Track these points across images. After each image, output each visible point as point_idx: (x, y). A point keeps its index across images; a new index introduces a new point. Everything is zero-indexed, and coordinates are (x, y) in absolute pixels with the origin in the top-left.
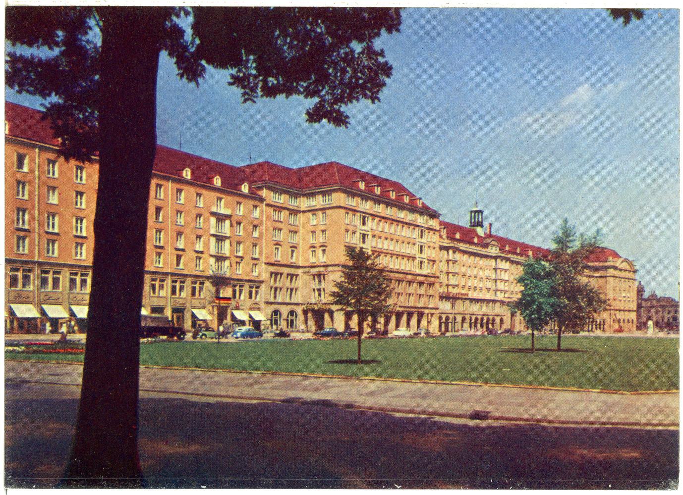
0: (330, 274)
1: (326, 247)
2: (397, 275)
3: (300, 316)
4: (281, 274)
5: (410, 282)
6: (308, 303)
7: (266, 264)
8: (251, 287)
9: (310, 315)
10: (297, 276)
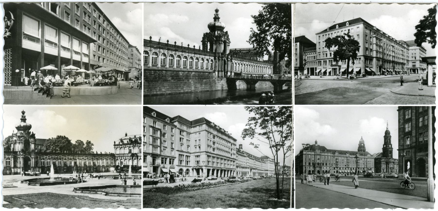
3: (191, 171)
4: (183, 155)
5: (228, 160)
8: (170, 159)
10: (190, 156)
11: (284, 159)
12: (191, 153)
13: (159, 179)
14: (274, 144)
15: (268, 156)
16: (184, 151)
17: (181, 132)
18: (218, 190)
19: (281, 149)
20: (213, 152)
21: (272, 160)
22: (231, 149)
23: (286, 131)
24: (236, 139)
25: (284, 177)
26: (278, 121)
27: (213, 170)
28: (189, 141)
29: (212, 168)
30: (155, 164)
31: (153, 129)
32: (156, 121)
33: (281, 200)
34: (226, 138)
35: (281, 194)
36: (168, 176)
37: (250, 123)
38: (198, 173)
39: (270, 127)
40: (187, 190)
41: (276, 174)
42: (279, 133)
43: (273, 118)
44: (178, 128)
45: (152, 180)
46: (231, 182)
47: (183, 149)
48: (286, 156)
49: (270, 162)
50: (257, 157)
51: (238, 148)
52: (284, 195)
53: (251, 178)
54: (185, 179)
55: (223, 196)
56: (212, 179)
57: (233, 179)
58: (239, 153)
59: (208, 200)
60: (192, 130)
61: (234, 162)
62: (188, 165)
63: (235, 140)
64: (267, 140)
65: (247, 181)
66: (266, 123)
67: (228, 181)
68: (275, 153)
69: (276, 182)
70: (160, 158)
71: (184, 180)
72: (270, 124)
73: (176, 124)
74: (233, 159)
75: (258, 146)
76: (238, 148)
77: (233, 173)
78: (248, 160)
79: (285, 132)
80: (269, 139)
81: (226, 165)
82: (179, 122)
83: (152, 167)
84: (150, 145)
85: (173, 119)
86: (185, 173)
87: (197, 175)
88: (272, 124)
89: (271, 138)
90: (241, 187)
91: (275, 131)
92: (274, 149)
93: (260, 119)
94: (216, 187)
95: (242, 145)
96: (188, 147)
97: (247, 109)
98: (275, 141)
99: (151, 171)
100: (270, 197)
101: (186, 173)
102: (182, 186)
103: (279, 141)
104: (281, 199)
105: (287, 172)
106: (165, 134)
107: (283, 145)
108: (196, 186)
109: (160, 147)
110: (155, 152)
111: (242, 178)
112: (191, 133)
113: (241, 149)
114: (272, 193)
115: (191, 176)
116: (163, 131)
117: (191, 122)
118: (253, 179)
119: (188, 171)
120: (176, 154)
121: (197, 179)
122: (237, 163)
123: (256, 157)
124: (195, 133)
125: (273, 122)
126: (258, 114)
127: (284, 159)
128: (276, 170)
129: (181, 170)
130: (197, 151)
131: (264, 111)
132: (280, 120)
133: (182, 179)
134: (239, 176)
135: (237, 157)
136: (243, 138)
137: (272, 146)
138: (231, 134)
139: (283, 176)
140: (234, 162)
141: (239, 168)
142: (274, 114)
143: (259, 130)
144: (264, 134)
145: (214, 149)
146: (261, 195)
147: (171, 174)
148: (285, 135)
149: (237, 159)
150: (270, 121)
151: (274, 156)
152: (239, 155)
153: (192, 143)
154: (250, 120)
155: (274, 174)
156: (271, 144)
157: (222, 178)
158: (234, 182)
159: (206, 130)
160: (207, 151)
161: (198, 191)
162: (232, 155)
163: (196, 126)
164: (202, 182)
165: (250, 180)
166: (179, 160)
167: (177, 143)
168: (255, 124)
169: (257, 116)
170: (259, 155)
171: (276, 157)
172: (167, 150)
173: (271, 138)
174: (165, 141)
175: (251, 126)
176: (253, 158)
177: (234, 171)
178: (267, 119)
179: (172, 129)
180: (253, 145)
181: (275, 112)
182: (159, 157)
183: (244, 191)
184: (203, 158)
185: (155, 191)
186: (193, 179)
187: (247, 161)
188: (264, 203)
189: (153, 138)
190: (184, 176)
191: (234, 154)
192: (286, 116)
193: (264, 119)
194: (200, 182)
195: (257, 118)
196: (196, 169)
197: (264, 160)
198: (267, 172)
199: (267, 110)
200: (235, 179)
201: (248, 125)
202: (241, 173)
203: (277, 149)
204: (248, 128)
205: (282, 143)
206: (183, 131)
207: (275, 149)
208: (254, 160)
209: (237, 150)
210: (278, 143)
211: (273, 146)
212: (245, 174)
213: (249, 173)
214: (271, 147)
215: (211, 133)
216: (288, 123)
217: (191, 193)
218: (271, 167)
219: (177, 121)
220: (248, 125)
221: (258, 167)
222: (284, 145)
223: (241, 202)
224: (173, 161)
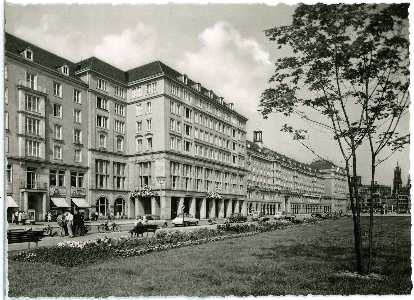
0: (157, 161)
1: (152, 135)
2: (216, 167)
5: (226, 173)
6: (135, 191)
7: (91, 150)
8: (73, 173)
9: (137, 200)
10: (124, 165)
11: (373, 167)
12: (127, 156)
13: (45, 226)
14: (344, 127)
15: (330, 159)
16: (110, 150)
17: (99, 99)
18: (201, 253)
19: (366, 140)
20: (185, 152)
21: (341, 172)
22: (234, 144)
23: (376, 92)
24: (248, 119)
25: (375, 214)
26: (355, 67)
27: (187, 201)
28: (123, 123)
29: (183, 195)
30: (34, 186)
31: (26, 95)
32: (33, 70)
33: (367, 277)
34: (218, 114)
35: (366, 261)
36: (70, 217)
37: (281, 74)
38: (147, 209)
39: (334, 83)
40: (118, 254)
41: (352, 207)
42: (357, 97)
44: (91, 91)
45: (27, 228)
46: (235, 230)
47: (105, 147)
48: (376, 158)
49: (337, 176)
50: (303, 165)
51: (252, 140)
52: (374, 263)
53: (286, 218)
54: (114, 225)
55: (214, 267)
56: (185, 224)
57: (239, 224)
59: (174, 279)
61: (241, 176)
62: (121, 189)
63: (243, 120)
64: (326, 119)
65: (276, 227)
67: (228, 229)
68: (348, 152)
69: (353, 228)
70: (47, 171)
71: (110, 228)
72: (334, 76)
73: (87, 79)
74: (239, 169)
75: (303, 134)
76: (251, 139)
77: (240, 208)
78: (277, 171)
79: (375, 96)
80: (332, 116)
81: (221, 187)
82: (95, 75)
83: (26, 197)
84: (19, 135)
85: (79, 66)
86: (113, 210)
88: (339, 76)
89: (337, 112)
90: (262, 242)
91: (348, 94)
92: (346, 142)
93: (306, 62)
94: (196, 244)
96: (119, 141)
97: (271, 36)
98: (347, 122)
99: (22, 205)
100: (337, 269)
101: (115, 208)
102: (105, 244)
103: (358, 119)
104: (367, 274)
105: (380, 202)
106: (59, 107)
107: (368, 131)
108: (143, 244)
109: (46, 141)
110: (32, 155)
111: (264, 220)
112: (126, 104)
113: (259, 144)
114: (344, 257)
115: (129, 216)
116: (53, 100)
117: (126, 74)
118: (293, 222)
119: (119, 205)
121: (143, 222)
122: (249, 181)
123: (298, 163)
124: (138, 102)
125: (341, 70)
126: (301, 48)
127: (373, 167)
128: (351, 197)
131: (317, 40)
132: (360, 64)
133: (106, 225)
134: (255, 216)
135: (249, 164)
136: (263, 114)
137: (339, 133)
138: (232, 104)
139: (371, 213)
140: (241, 176)
141: (254, 192)
142: (342, 47)
144: (319, 102)
145: (188, 144)
146: (313, 265)
147: (75, 212)
148: (375, 105)
149: (249, 169)
150: (333, 69)
151: (347, 161)
152: (254, 158)
154: (281, 67)
155: (348, 209)
156: (337, 128)
157: (210, 221)
158: (242, 229)
159: (165, 95)
160: (168, 150)
161: (149, 255)
162: (237, 159)
163: (138, 85)
164: (158, 231)
165: (285, 225)
166: (97, 175)
167: (89, 129)
168: (294, 77)
169: (300, 55)
170: (307, 158)
171: (351, 162)
172: (65, 147)
173: (337, 112)
174: (59, 126)
175: (285, 81)
176: (291, 166)
177: (242, 202)
178: (326, 63)
179: (77, 92)
180: (291, 131)
181: (345, 42)
182: (43, 168)
185: (35, 259)
186: (136, 225)
187: (277, 175)
188: (321, 286)
189: (26, 118)
190: (109, 218)
191: (241, 157)
192: (374, 52)
193: (318, 63)
194: (154, 231)
195: (300, 60)
196: (140, 198)
197: (321, 171)
198: (327, 202)
199: (324, 37)
200: (245, 224)
201: (275, 78)
202: (259, 206)
204: (276, 88)
205: (366, 126)
206: (107, 98)
207: (350, 141)
208: (293, 170)
209: (249, 146)
210: (357, 126)
211: (344, 134)
212: (271, 207)
213: (283, 206)
214: (337, 137)
216: (381, 73)
217: (127, 264)
220: (275, 78)
221: (305, 189)
223: (263, 283)
224: (80, 179)
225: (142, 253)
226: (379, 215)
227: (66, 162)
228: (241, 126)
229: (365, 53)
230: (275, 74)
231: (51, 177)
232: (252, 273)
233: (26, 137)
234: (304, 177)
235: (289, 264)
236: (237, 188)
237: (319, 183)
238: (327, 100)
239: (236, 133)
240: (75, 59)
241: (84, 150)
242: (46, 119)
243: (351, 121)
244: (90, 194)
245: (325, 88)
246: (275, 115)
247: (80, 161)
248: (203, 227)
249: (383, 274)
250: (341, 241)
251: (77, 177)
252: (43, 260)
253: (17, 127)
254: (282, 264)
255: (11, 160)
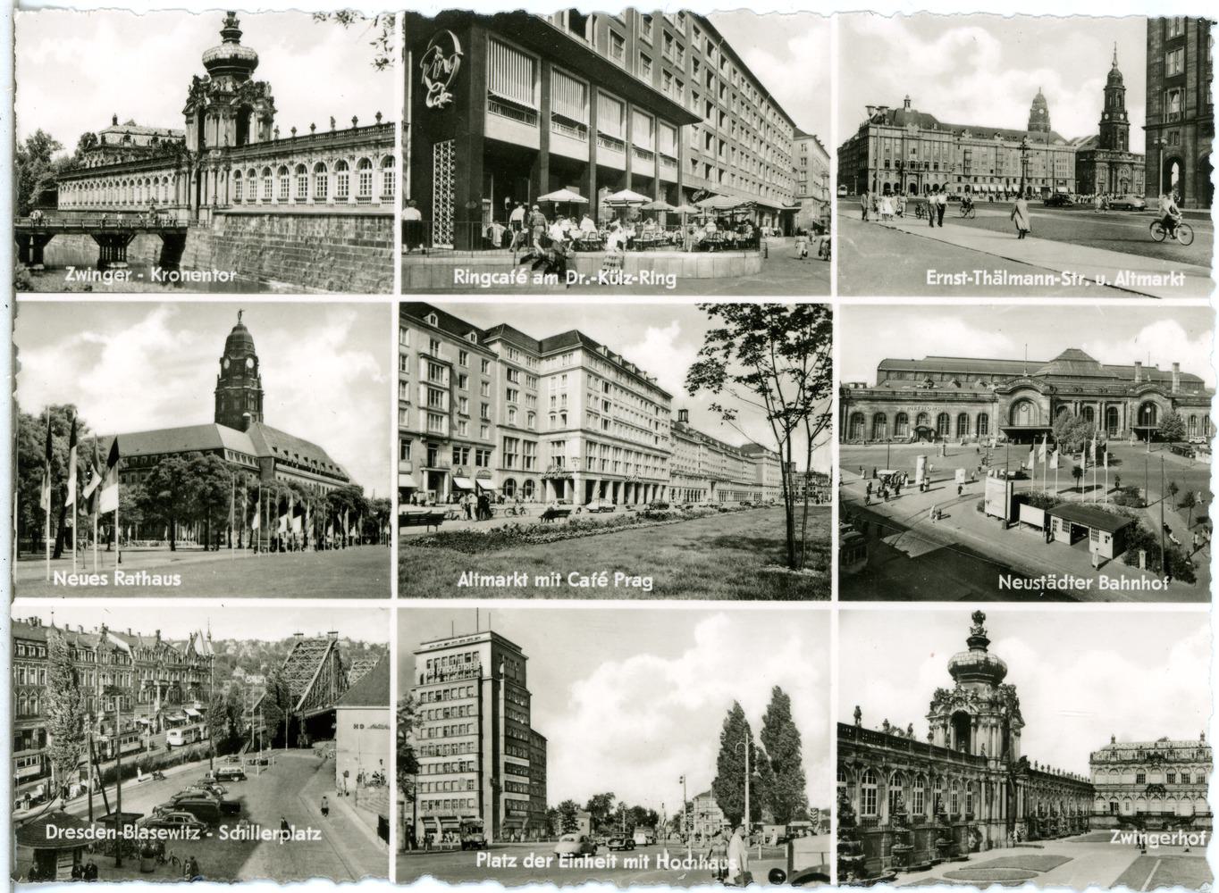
3: (539, 485)
8: (479, 452)
9: (548, 483)
10: (535, 443)
11: (810, 452)
12: (538, 434)
14: (779, 407)
15: (762, 443)
16: (519, 427)
17: (509, 371)
18: (618, 542)
19: (802, 423)
21: (774, 456)
22: (657, 423)
23: (814, 369)
25: (810, 504)
26: (792, 341)
27: (604, 484)
28: (535, 398)
29: (599, 479)
32: (438, 337)
33: (799, 573)
34: (642, 390)
35: (798, 555)
36: (474, 500)
37: (710, 347)
38: (560, 492)
39: (768, 358)
40: (526, 541)
41: (785, 495)
43: (777, 334)
44: (502, 361)
45: (426, 510)
46: (655, 517)
48: (814, 442)
49: (770, 461)
50: (732, 448)
52: (807, 558)
53: (712, 506)
54: (522, 509)
56: (604, 510)
58: (679, 435)
60: (545, 367)
62: (531, 469)
63: (667, 397)
64: (759, 398)
65: (701, 515)
66: (758, 346)
67: (648, 516)
68: (782, 435)
69: (785, 518)
70: (450, 448)
71: (518, 511)
72: (769, 350)
73: (496, 348)
75: (732, 414)
76: (676, 419)
77: (662, 494)
80: (765, 395)
81: (641, 470)
82: (505, 344)
83: (426, 475)
84: (420, 408)
85: (488, 334)
87: (558, 497)
88: (775, 350)
89: (771, 391)
91: (784, 371)
92: (780, 424)
93: (739, 334)
94: (612, 532)
95: (686, 411)
98: (782, 401)
100: (767, 563)
101: (524, 491)
102: (512, 530)
103: (794, 399)
105: (816, 491)
106: (465, 378)
107: (805, 412)
108: (554, 531)
109: (450, 415)
111: (688, 507)
112: (539, 376)
113: (684, 424)
114: (775, 550)
116: (458, 370)
117: (540, 343)
120: (495, 436)
121: (556, 507)
122: (672, 465)
123: (727, 446)
125: (777, 345)
126: (733, 319)
127: (810, 452)
128: (784, 485)
129: (510, 481)
130: (558, 429)
131: (752, 311)
132: (798, 338)
133: (514, 509)
134: (679, 502)
136: (690, 390)
137: (773, 414)
138: (656, 379)
139: (806, 502)
142: (779, 320)
143: (736, 367)
144: (752, 379)
145: (606, 422)
146: (740, 558)
147: (480, 494)
148: (813, 384)
149: (672, 450)
150: (768, 343)
152: (678, 439)
153: (544, 406)
154: (711, 339)
156: (771, 408)
157: (628, 507)
158: (664, 517)
159: (583, 368)
160: (584, 428)
162: (660, 441)
164: (570, 517)
165: (711, 514)
166: (505, 454)
168: (725, 351)
169: (732, 327)
170: (737, 441)
171: (785, 446)
172: (469, 423)
173: (771, 391)
174: (465, 399)
176: (719, 449)
177: (664, 487)
178: (761, 337)
179: (485, 362)
180: (720, 410)
181: (783, 314)
182: (446, 445)
183: (693, 545)
184: (574, 448)
185: (434, 544)
188: (749, 581)
191: (665, 438)
193: (752, 336)
195: (731, 333)
196: (552, 480)
197: (752, 455)
198: (758, 489)
200: (666, 511)
201: (704, 352)
203: (788, 423)
205: (802, 407)
207: (784, 422)
210: (793, 406)
211: (778, 415)
213: (709, 492)
215: (598, 377)
216: (820, 349)
218: (772, 474)
219: (499, 340)
220: (704, 352)
222: (809, 412)
223: (685, 576)
224: (486, 458)
225: (553, 541)
226: (815, 505)
227: (470, 439)
228: (665, 404)
229: (804, 326)
230: (703, 347)
231: (454, 454)
232: (673, 564)
233: (428, 410)
234: (733, 461)
235: (714, 556)
236: (659, 472)
237: (750, 469)
238: (760, 377)
239: (660, 411)
240: (484, 327)
241: (490, 427)
242: (450, 391)
243: (786, 402)
244: (496, 475)
245: (759, 364)
246: (705, 394)
247: (488, 437)
248: (620, 514)
249: (817, 569)
250: (771, 533)
251: (483, 455)
252: (443, 545)
253: (418, 399)
254: (706, 556)
255: (406, 439)
